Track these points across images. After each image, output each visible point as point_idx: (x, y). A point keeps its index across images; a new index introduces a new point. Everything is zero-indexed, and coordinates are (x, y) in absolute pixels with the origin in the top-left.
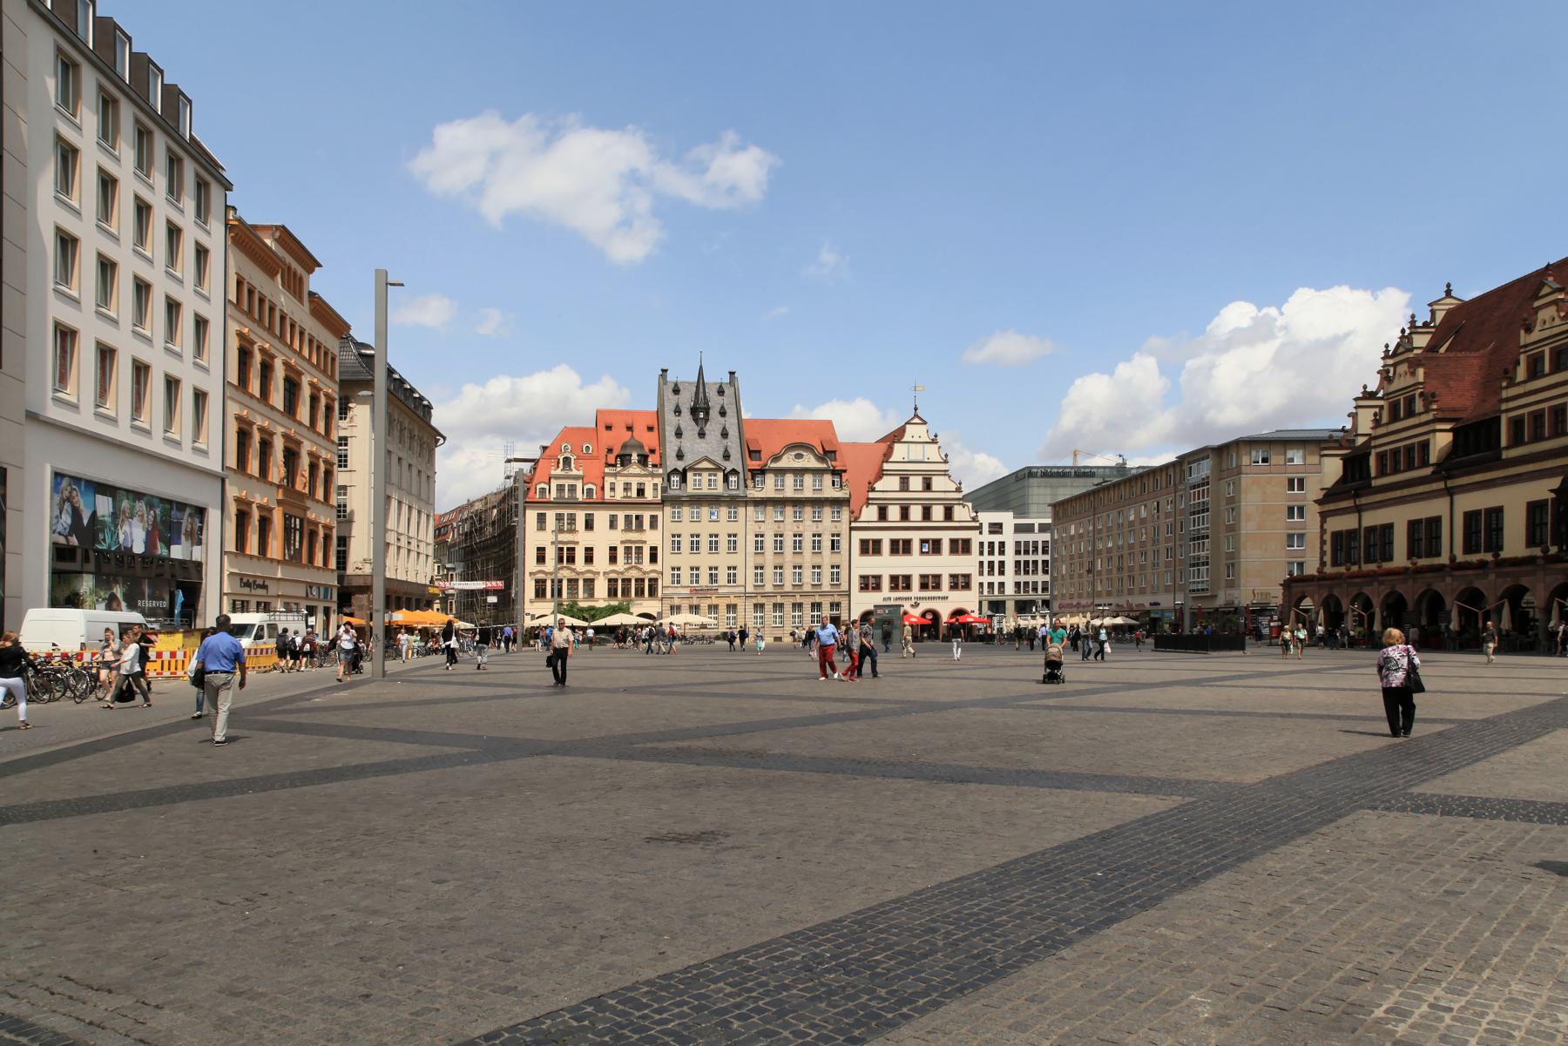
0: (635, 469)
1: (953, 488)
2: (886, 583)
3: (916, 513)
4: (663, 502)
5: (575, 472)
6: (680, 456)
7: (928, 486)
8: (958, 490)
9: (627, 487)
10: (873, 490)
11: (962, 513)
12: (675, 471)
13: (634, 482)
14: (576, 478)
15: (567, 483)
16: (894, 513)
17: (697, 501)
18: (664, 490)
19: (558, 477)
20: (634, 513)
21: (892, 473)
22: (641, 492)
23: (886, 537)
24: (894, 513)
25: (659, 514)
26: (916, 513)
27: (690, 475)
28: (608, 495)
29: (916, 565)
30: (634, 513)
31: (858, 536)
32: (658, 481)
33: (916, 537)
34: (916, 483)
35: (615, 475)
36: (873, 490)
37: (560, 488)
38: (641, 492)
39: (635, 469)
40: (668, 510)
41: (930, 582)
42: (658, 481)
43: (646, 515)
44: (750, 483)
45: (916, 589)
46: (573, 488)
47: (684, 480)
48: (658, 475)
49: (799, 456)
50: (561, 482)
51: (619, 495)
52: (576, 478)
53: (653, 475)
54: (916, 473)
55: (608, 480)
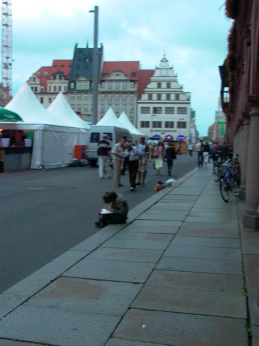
0: (57, 81)
1: (179, 87)
2: (151, 124)
3: (164, 97)
5: (36, 82)
7: (169, 86)
8: (181, 88)
9: (55, 88)
10: (146, 88)
11: (182, 97)
13: (58, 85)
14: (37, 84)
16: (155, 97)
17: (80, 92)
21: (154, 81)
23: (152, 106)
24: (155, 97)
26: (164, 97)
27: (77, 82)
28: (48, 91)
29: (163, 117)
31: (140, 106)
32: (66, 85)
33: (164, 106)
34: (164, 85)
35: (50, 83)
36: (146, 88)
39: (57, 81)
41: (169, 124)
44: (99, 85)
45: (163, 128)
47: (75, 85)
49: (118, 75)
51: (52, 91)
52: (37, 84)
53: (65, 83)
54: (164, 81)
55: (49, 85)
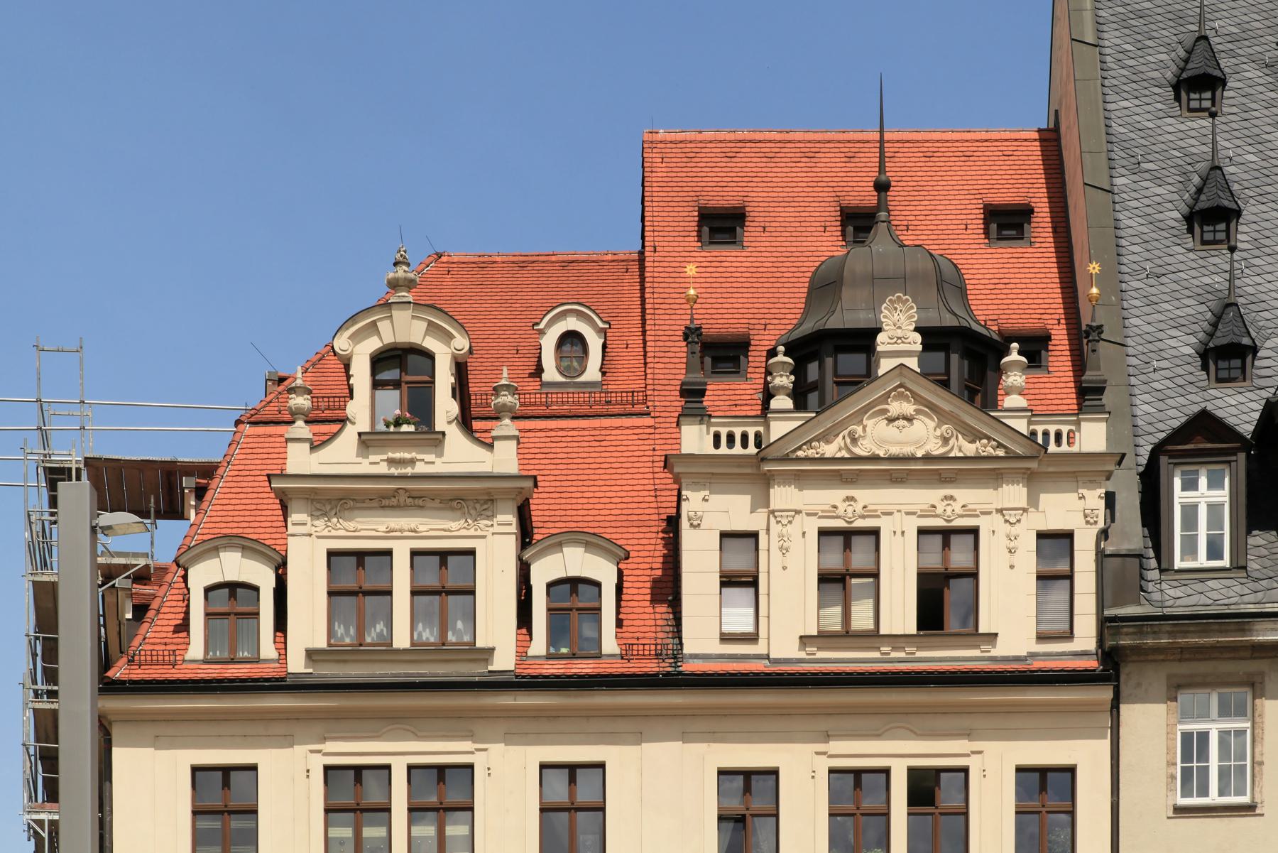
4: (1114, 668)
6: (1227, 354)
12: (1200, 438)
15: (401, 535)
18: (1118, 574)
19: (334, 498)
20: (899, 754)
22: (943, 598)
25: (1086, 755)
30: (899, 754)
37: (356, 579)
38: (943, 598)
40: (1149, 724)
42: (1074, 509)
43: (993, 777)
46: (446, 580)
48: (1079, 470)
50: (364, 531)
55: (712, 513)
